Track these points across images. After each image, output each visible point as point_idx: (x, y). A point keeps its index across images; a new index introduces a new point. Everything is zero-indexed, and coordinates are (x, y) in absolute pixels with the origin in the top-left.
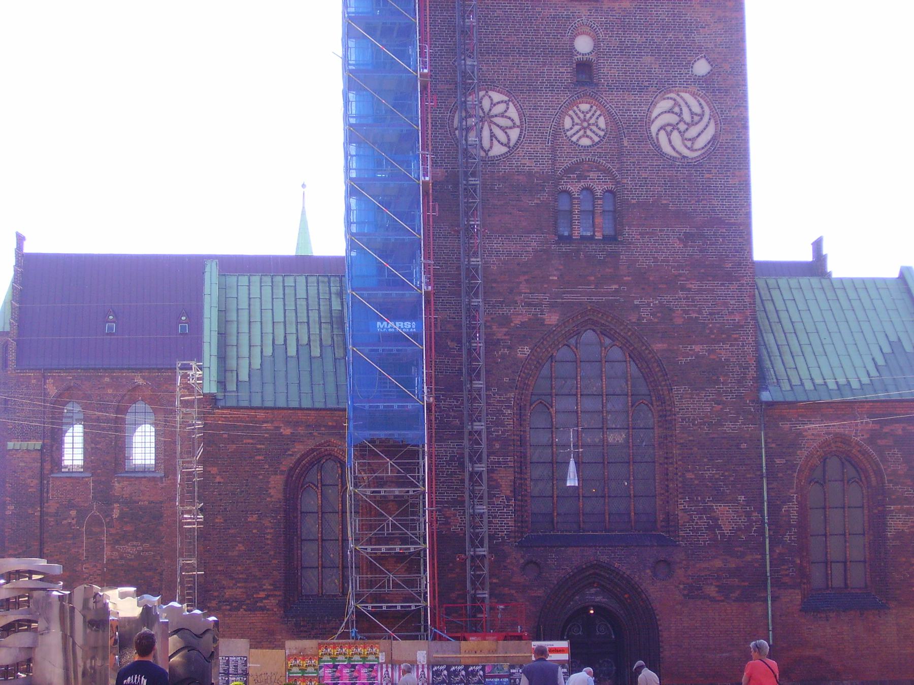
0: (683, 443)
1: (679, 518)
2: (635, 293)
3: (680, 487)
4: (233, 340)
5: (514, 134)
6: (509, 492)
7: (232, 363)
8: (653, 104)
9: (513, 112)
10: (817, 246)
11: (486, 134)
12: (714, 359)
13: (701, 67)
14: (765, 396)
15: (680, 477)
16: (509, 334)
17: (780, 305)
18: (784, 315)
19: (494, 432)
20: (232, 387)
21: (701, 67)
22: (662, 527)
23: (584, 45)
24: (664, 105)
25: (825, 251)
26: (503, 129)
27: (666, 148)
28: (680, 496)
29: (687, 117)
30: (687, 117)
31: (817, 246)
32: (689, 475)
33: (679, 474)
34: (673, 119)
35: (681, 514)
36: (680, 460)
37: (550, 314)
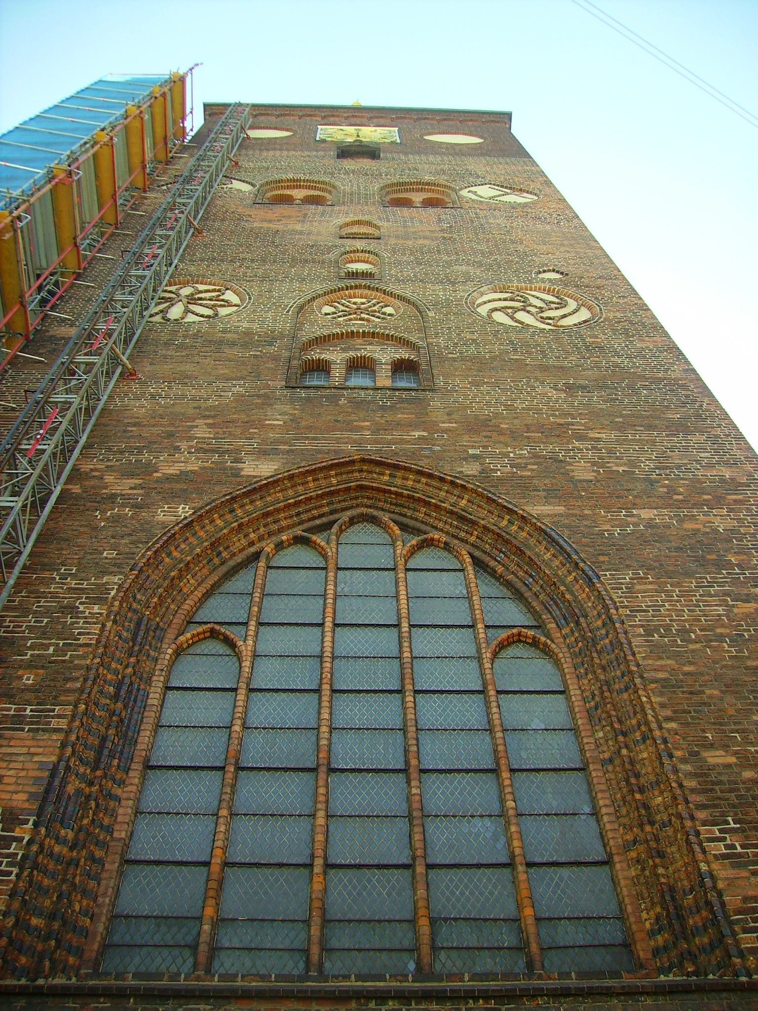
0: (665, 680)
1: (721, 885)
2: (466, 442)
3: (693, 791)
6: (23, 796)
12: (698, 530)
15: (684, 760)
16: (142, 488)
19: (32, 648)
22: (656, 952)
28: (701, 815)
32: (715, 757)
33: (678, 753)
35: (723, 872)
36: (668, 719)
37: (257, 463)
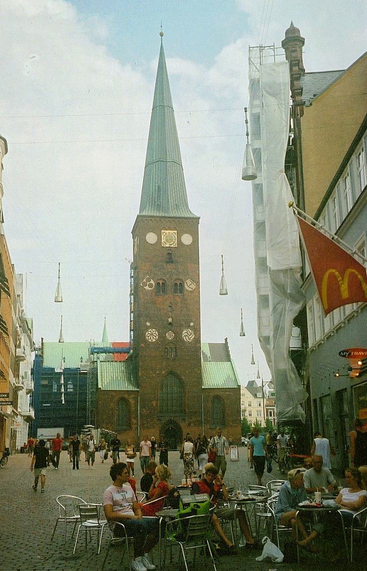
4: (103, 376)
5: (157, 337)
7: (103, 381)
8: (183, 331)
9: (157, 333)
10: (226, 339)
11: (152, 337)
13: (192, 324)
14: (203, 387)
17: (207, 368)
18: (208, 370)
20: (104, 386)
21: (192, 324)
23: (170, 320)
24: (185, 331)
25: (228, 341)
26: (155, 336)
27: (185, 340)
29: (189, 333)
30: (189, 333)
31: (226, 339)
34: (187, 334)
